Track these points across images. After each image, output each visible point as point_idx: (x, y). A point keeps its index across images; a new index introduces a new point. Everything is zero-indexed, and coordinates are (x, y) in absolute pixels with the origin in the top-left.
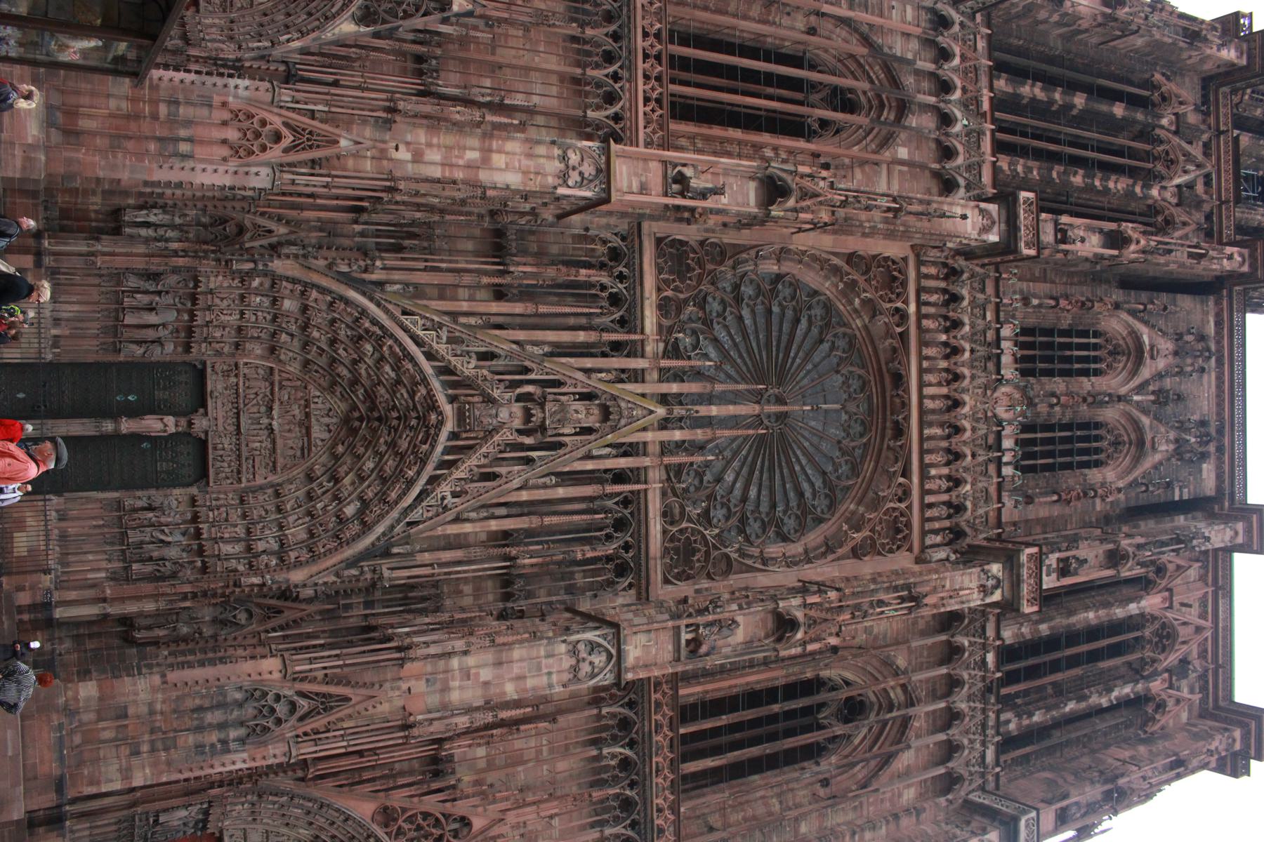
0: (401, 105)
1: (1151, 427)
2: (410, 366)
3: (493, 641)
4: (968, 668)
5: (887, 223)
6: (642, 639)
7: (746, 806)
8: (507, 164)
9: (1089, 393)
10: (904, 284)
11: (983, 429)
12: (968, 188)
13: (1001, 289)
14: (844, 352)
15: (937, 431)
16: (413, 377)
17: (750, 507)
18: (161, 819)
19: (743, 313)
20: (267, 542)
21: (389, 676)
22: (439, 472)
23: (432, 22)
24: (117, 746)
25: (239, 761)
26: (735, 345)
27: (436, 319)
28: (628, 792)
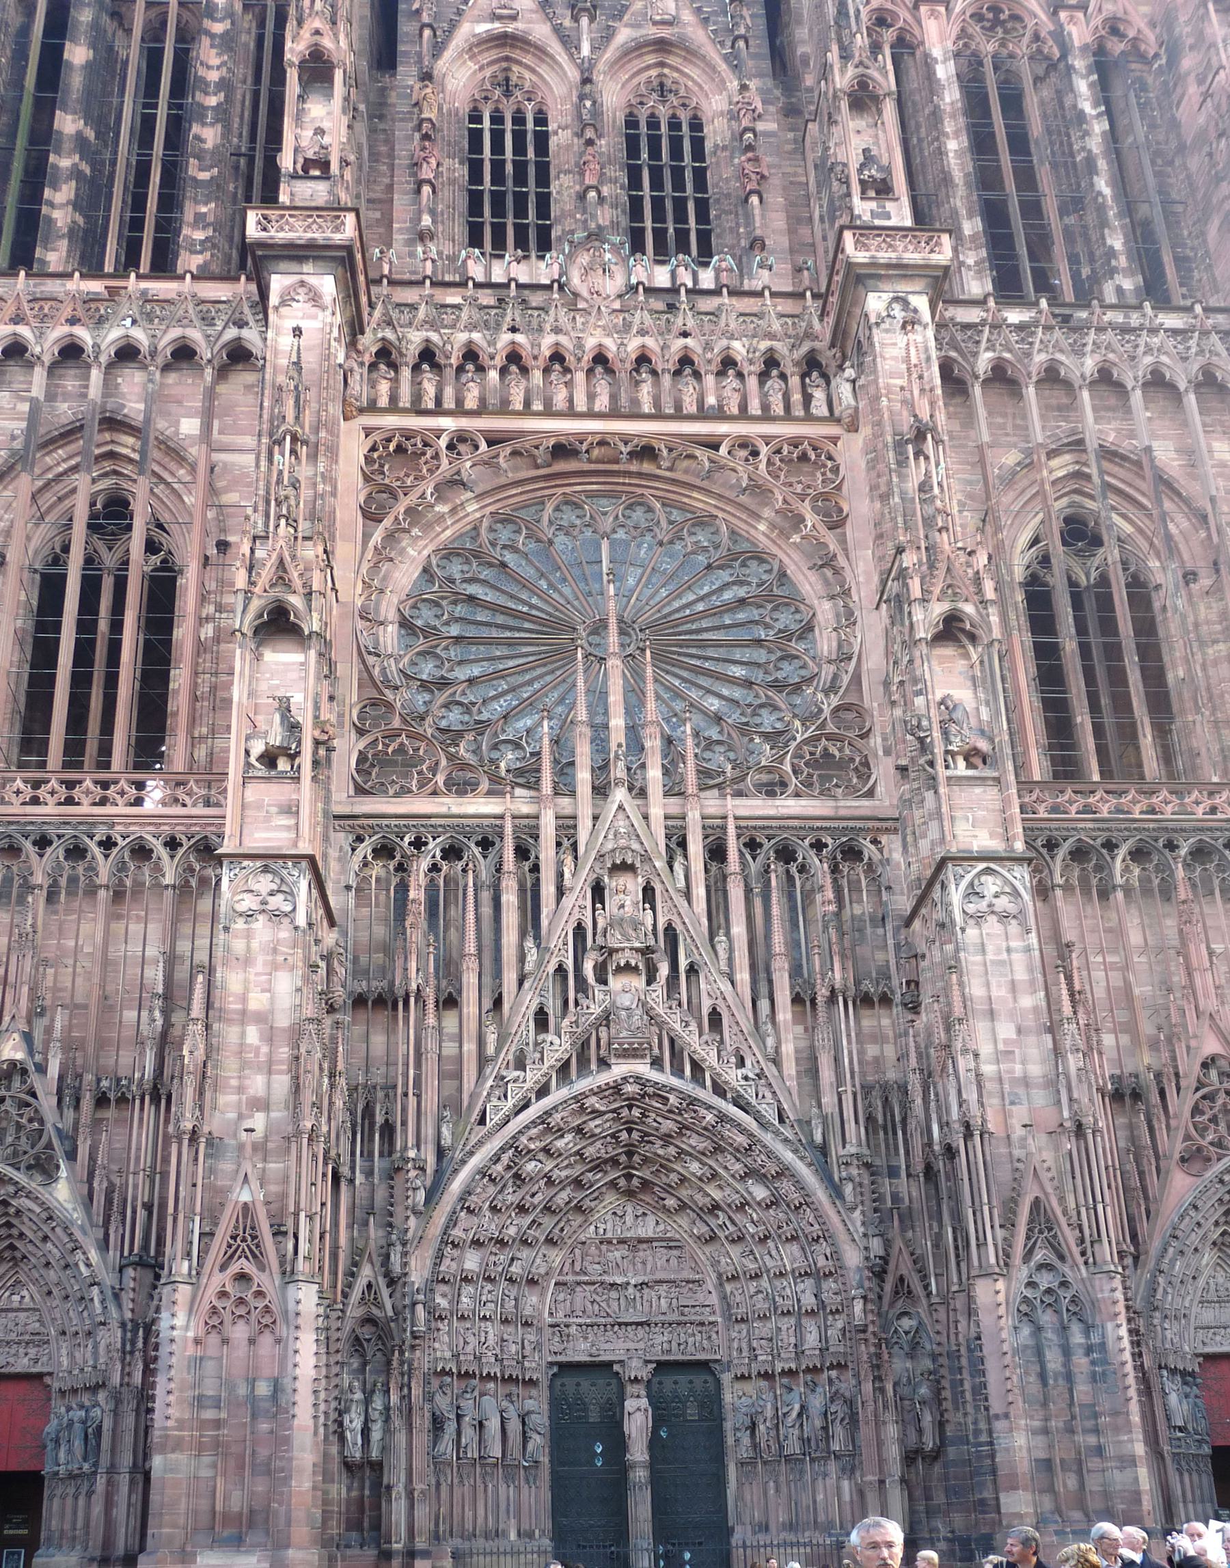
1: (636, 26)
4: (1028, 355)
5: (316, 456)
7: (1216, 692)
9: (580, 134)
11: (640, 318)
12: (241, 324)
13: (407, 277)
14: (518, 532)
15: (645, 392)
16: (573, 1112)
17: (758, 676)
18: (1180, 1423)
19: (463, 678)
22: (708, 1083)
23: (45, 1088)
26: (512, 690)
27: (490, 1083)
28: (1183, 852)
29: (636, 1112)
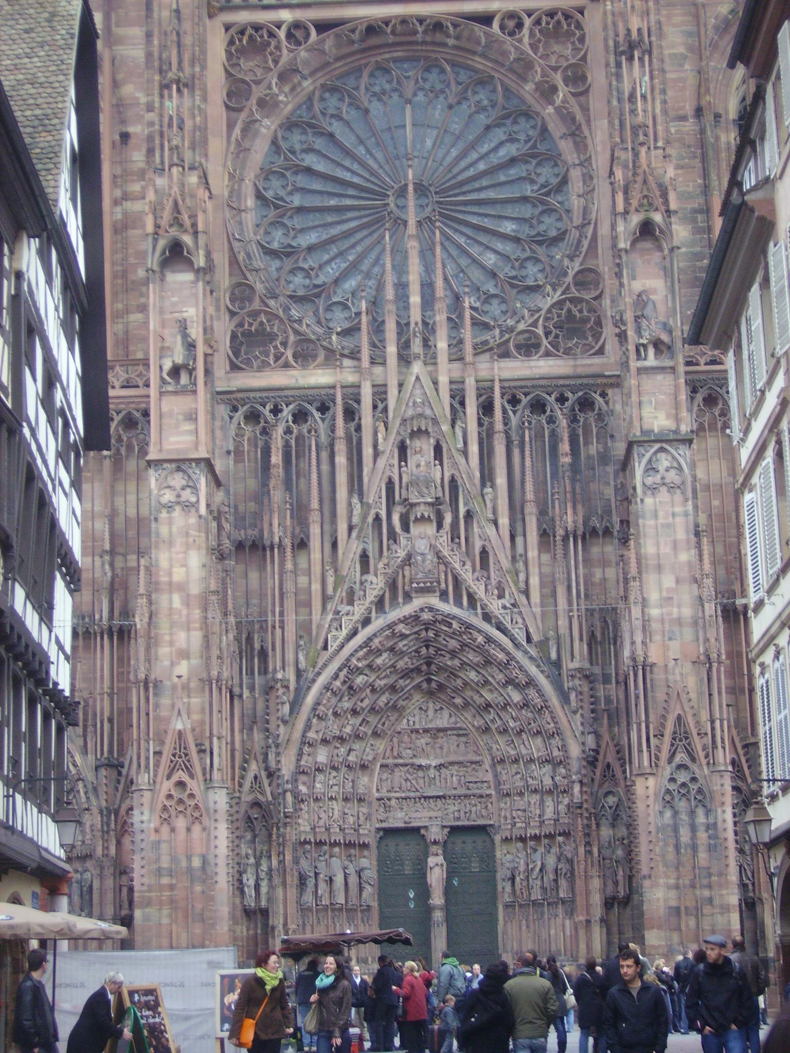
0: (142, 676)
2: (376, 641)
3: (634, 579)
6: (647, 412)
8: (182, 566)
10: (257, 28)
14: (342, 100)
16: (387, 637)
20: (544, 776)
21: (662, 676)
22: (479, 611)
24: (702, 915)
25: (726, 815)
27: (330, 616)
29: (431, 634)
